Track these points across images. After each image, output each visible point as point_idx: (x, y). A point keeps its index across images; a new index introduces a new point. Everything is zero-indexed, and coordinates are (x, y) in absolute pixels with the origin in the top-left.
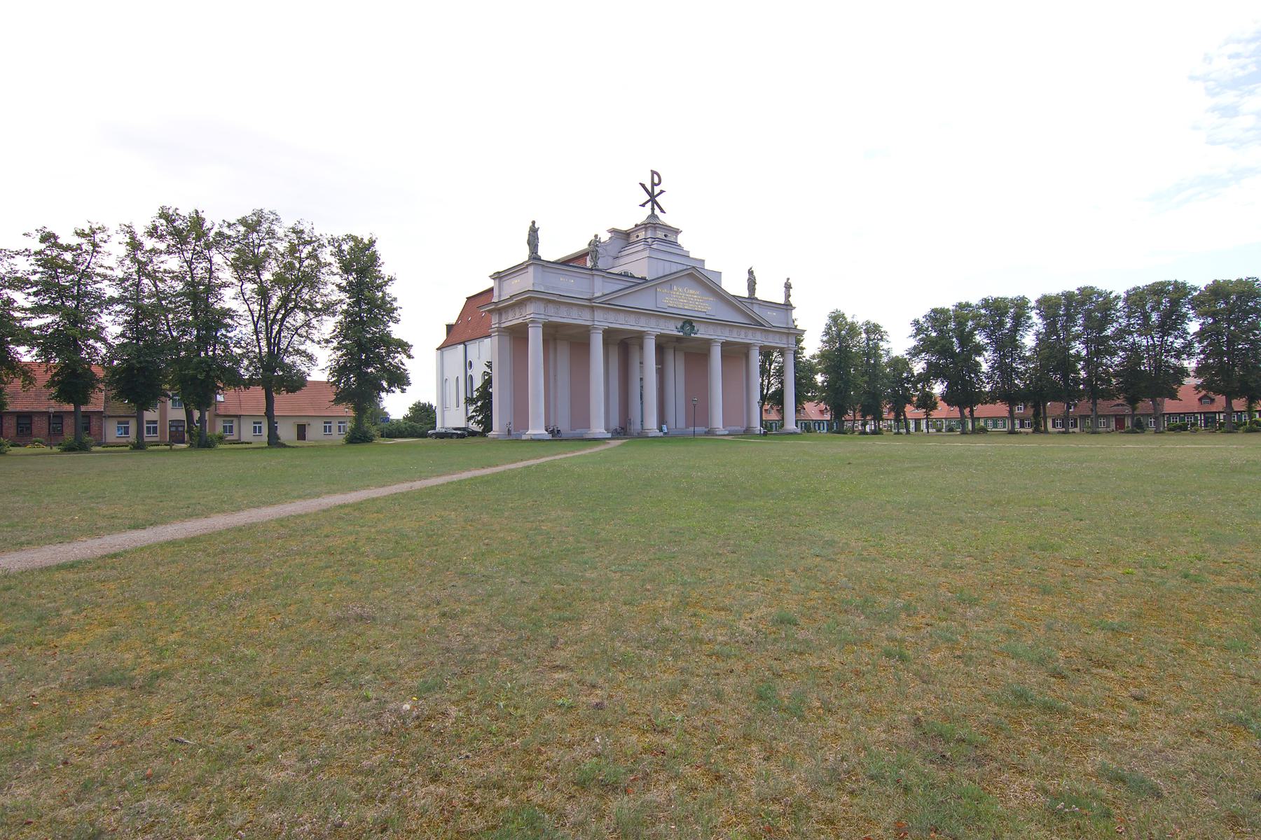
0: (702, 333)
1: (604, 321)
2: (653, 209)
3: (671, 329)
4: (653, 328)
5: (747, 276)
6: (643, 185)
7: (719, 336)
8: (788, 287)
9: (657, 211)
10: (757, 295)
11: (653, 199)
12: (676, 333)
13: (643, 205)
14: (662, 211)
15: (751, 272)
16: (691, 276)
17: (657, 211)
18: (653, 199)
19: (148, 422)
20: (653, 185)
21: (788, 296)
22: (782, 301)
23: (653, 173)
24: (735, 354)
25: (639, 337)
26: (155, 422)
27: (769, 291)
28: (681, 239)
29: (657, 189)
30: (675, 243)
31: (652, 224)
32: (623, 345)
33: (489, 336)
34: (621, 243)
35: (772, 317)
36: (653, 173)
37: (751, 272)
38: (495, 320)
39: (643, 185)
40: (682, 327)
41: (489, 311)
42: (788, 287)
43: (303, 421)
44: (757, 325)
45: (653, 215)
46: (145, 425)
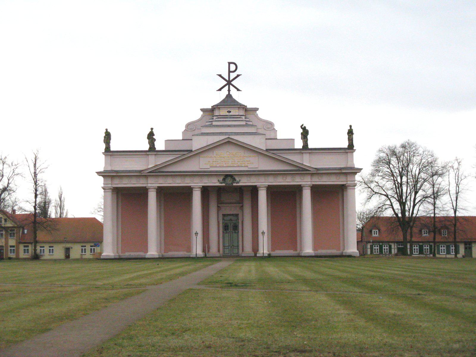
0: (244, 182)
1: (153, 184)
2: (229, 90)
3: (214, 182)
4: (197, 184)
6: (220, 76)
7: (262, 183)
8: (350, 133)
10: (310, 146)
11: (229, 83)
12: (218, 184)
13: (220, 90)
16: (229, 143)
18: (229, 83)
19: (11, 247)
20: (230, 72)
21: (351, 140)
25: (187, 192)
26: (13, 246)
29: (233, 75)
32: (175, 199)
34: (208, 118)
42: (350, 133)
43: (68, 245)
44: (302, 171)
45: (229, 96)
46: (9, 248)
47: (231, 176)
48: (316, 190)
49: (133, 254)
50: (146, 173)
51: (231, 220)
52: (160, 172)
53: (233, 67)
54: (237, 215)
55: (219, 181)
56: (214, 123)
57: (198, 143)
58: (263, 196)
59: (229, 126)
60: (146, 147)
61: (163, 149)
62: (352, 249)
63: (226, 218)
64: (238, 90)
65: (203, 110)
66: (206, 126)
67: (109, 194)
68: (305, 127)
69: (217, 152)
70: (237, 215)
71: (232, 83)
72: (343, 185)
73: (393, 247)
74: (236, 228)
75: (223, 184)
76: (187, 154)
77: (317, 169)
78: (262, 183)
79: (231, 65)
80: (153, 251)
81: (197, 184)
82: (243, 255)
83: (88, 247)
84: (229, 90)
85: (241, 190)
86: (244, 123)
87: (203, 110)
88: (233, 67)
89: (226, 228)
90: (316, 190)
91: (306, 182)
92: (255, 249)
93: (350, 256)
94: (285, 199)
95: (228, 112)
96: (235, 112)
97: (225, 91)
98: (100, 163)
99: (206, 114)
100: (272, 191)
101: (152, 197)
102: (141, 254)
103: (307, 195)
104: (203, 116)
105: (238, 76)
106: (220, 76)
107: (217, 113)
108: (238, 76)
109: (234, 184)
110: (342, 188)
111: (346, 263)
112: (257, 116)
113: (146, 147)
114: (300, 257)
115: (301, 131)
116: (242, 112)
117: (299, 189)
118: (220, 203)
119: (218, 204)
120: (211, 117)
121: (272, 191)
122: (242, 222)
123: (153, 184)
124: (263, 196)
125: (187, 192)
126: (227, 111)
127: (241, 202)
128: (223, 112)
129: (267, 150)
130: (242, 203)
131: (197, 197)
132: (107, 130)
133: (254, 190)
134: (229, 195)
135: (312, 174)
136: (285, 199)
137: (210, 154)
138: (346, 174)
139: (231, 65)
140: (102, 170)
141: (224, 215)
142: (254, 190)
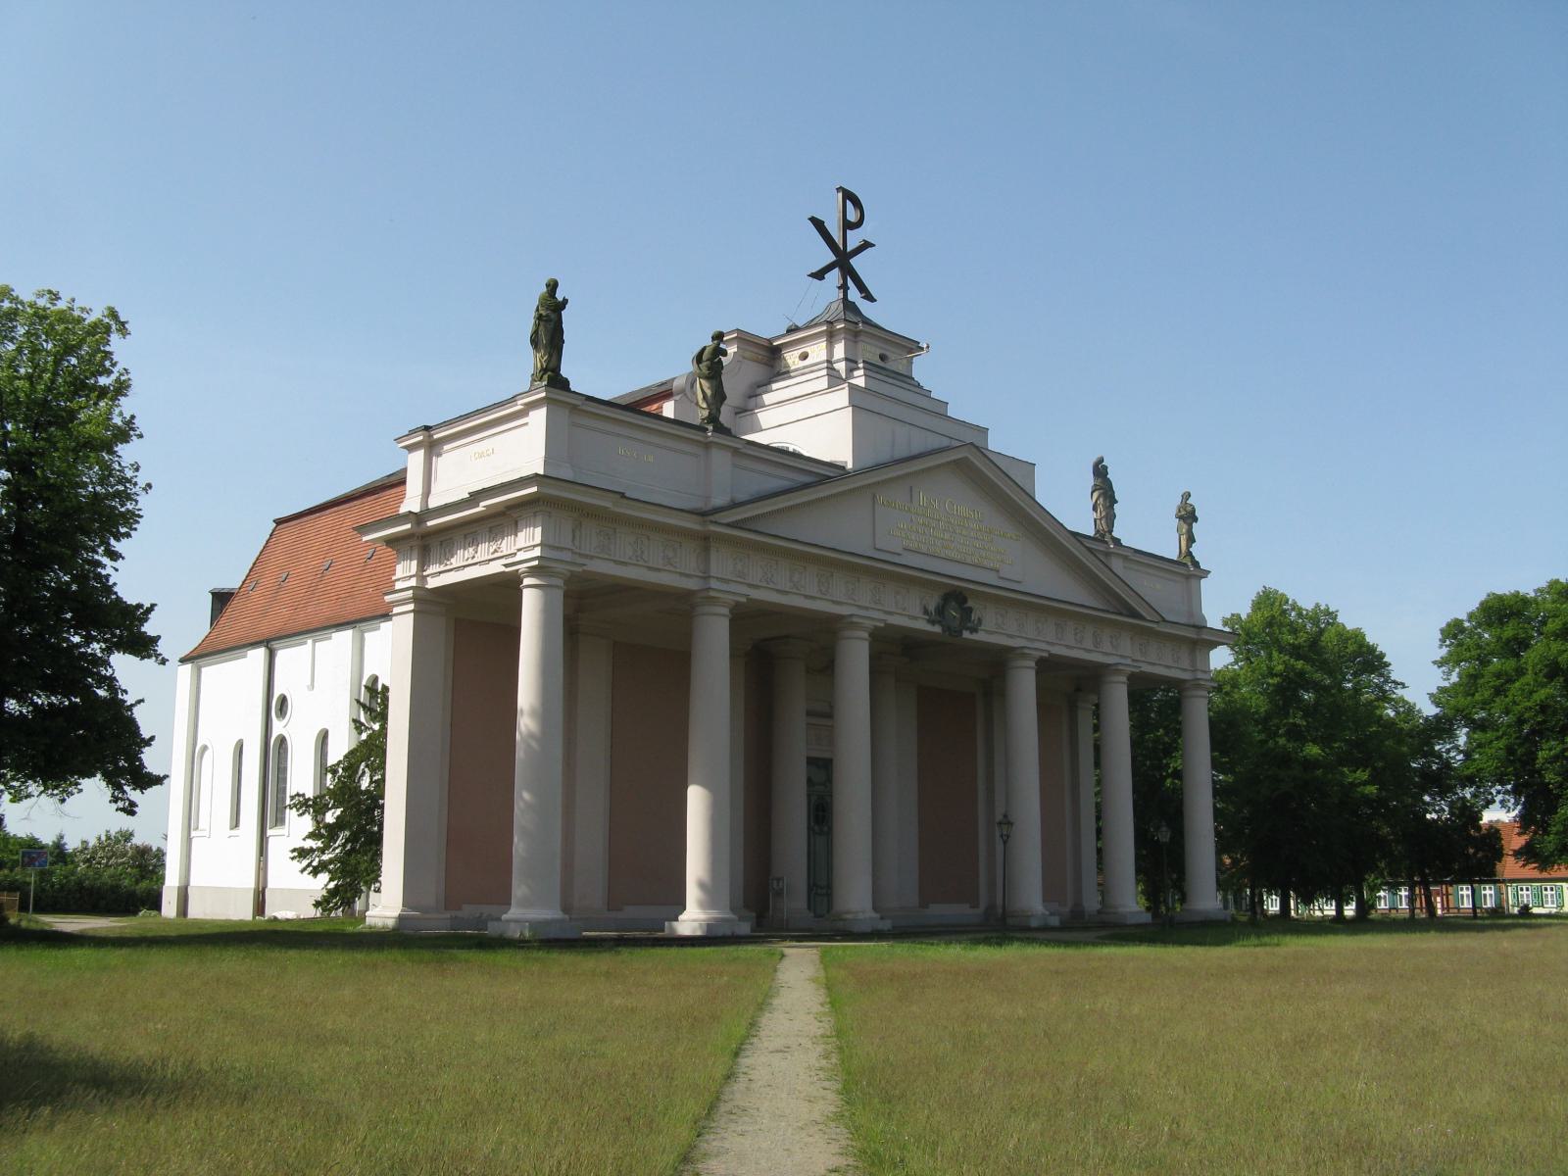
0: (993, 629)
2: (844, 287)
3: (910, 614)
5: (1090, 480)
6: (818, 224)
8: (1188, 516)
9: (854, 294)
11: (843, 261)
13: (819, 275)
14: (869, 297)
18: (843, 261)
20: (848, 226)
22: (1170, 550)
23: (849, 196)
24: (1070, 687)
25: (819, 639)
27: (1146, 529)
28: (922, 370)
29: (854, 239)
30: (906, 379)
32: (779, 658)
33: (386, 616)
35: (1153, 590)
37: (1100, 471)
38: (405, 572)
39: (818, 224)
40: (941, 611)
41: (391, 541)
42: (1188, 516)
50: (728, 525)
55: (926, 612)
68: (1105, 468)
71: (854, 261)
75: (937, 629)
77: (1164, 620)
84: (844, 287)
95: (883, 357)
99: (747, 354)
109: (966, 634)
126: (879, 352)
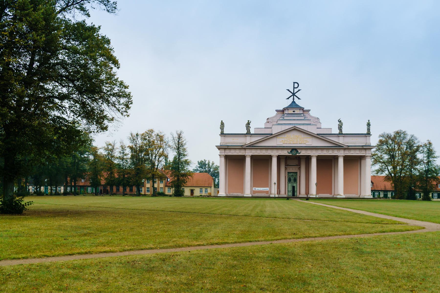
0: (303, 153)
1: (249, 153)
2: (294, 99)
3: (285, 153)
4: (275, 153)
6: (288, 90)
7: (314, 154)
8: (369, 125)
11: (294, 94)
13: (288, 98)
15: (340, 121)
16: (295, 129)
17: (296, 100)
18: (294, 94)
20: (294, 88)
21: (369, 130)
23: (294, 83)
25: (270, 158)
29: (296, 90)
31: (294, 105)
32: (261, 163)
34: (280, 115)
36: (294, 83)
40: (291, 151)
42: (369, 125)
43: (193, 188)
44: (339, 147)
45: (294, 102)
47: (296, 149)
48: (347, 159)
49: (235, 194)
51: (292, 175)
52: (252, 146)
53: (296, 85)
54: (296, 173)
56: (285, 118)
57: (276, 130)
58: (314, 162)
59: (294, 120)
60: (245, 132)
61: (254, 133)
62: (368, 193)
63: (289, 174)
64: (299, 99)
65: (277, 111)
66: (281, 120)
67: (223, 159)
69: (287, 135)
70: (296, 173)
72: (361, 156)
73: (381, 193)
74: (295, 180)
75: (291, 154)
76: (270, 136)
77: (348, 146)
78: (314, 154)
79: (295, 84)
80: (222, 193)
81: (275, 153)
82: (300, 196)
83: (204, 190)
84: (294, 99)
85: (299, 158)
86: (303, 118)
87: (277, 111)
88: (296, 85)
89: (289, 180)
90: (347, 159)
91: (341, 153)
92: (307, 192)
93: (364, 199)
94: (327, 163)
96: (297, 111)
97: (291, 100)
98: (218, 140)
100: (320, 159)
101: (248, 161)
102: (240, 194)
103: (341, 161)
104: (277, 114)
105: (299, 90)
106: (288, 90)
107: (286, 112)
108: (299, 90)
109: (297, 154)
110: (361, 158)
111: (365, 204)
112: (309, 115)
113: (245, 132)
114: (334, 199)
115: (338, 123)
116: (301, 112)
117: (335, 158)
118: (287, 165)
119: (285, 166)
120: (282, 115)
121: (320, 159)
122: (300, 177)
123: (249, 153)
124: (314, 162)
125: (270, 158)
127: (299, 165)
128: (291, 111)
129: (317, 134)
130: (300, 166)
131: (274, 161)
132: (222, 121)
133: (308, 159)
134: (294, 161)
135: (345, 149)
136: (327, 163)
137: (283, 136)
138: (366, 149)
139: (295, 84)
140: (219, 145)
141: (288, 173)
142: (308, 159)
